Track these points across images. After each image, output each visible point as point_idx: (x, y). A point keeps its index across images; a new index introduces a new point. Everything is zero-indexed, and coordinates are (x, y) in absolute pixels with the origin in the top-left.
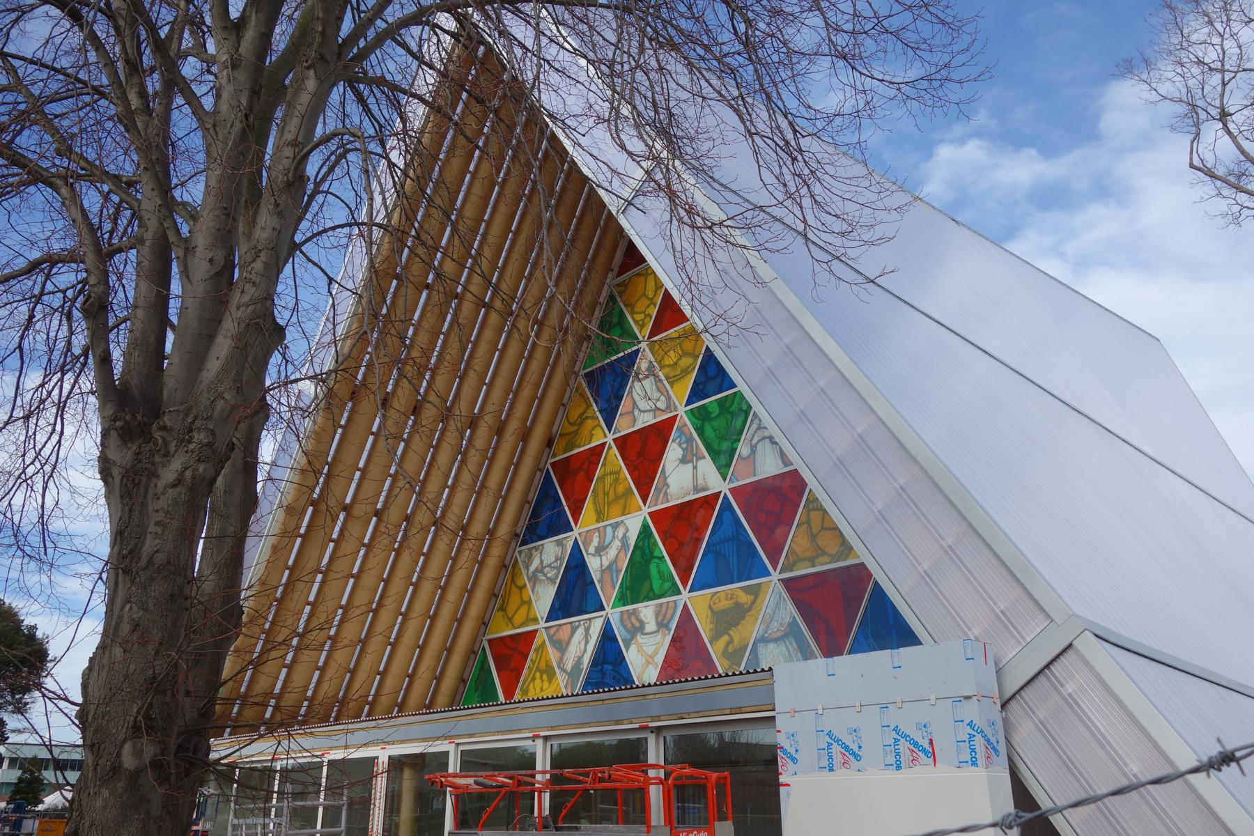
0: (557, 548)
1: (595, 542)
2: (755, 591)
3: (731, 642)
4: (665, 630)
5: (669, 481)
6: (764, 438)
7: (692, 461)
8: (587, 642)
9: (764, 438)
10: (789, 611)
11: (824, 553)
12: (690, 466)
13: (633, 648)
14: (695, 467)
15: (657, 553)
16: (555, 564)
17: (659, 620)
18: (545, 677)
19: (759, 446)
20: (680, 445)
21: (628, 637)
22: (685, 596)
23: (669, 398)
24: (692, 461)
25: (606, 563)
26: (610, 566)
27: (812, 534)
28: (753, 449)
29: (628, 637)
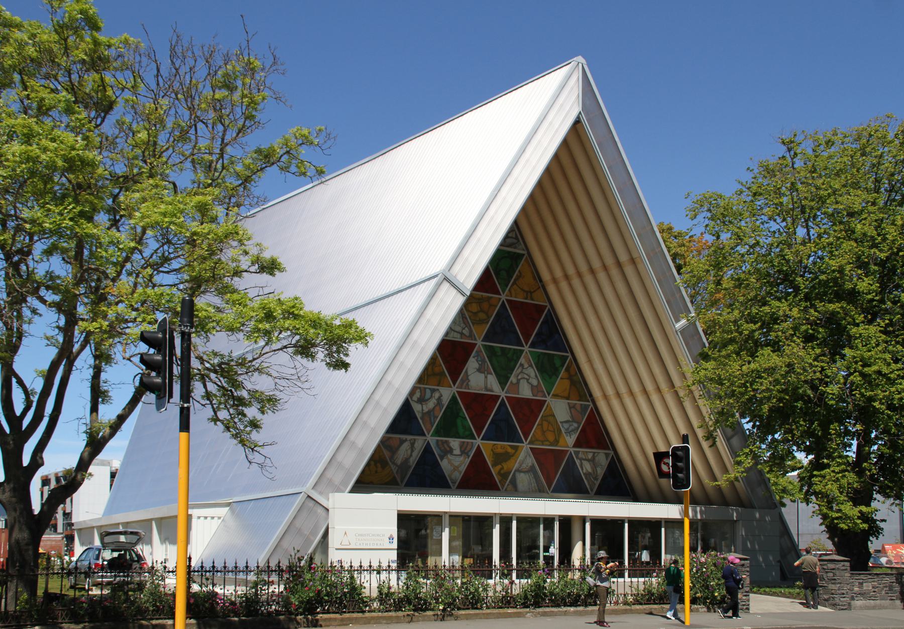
3: (502, 468)
5: (470, 378)
6: (524, 378)
7: (484, 373)
8: (412, 451)
9: (524, 378)
10: (531, 461)
11: (548, 441)
12: (483, 375)
14: (486, 377)
15: (461, 414)
18: (379, 465)
19: (521, 381)
20: (477, 361)
21: (442, 454)
22: (478, 442)
23: (471, 331)
25: (426, 409)
26: (429, 412)
28: (518, 381)
29: (442, 454)
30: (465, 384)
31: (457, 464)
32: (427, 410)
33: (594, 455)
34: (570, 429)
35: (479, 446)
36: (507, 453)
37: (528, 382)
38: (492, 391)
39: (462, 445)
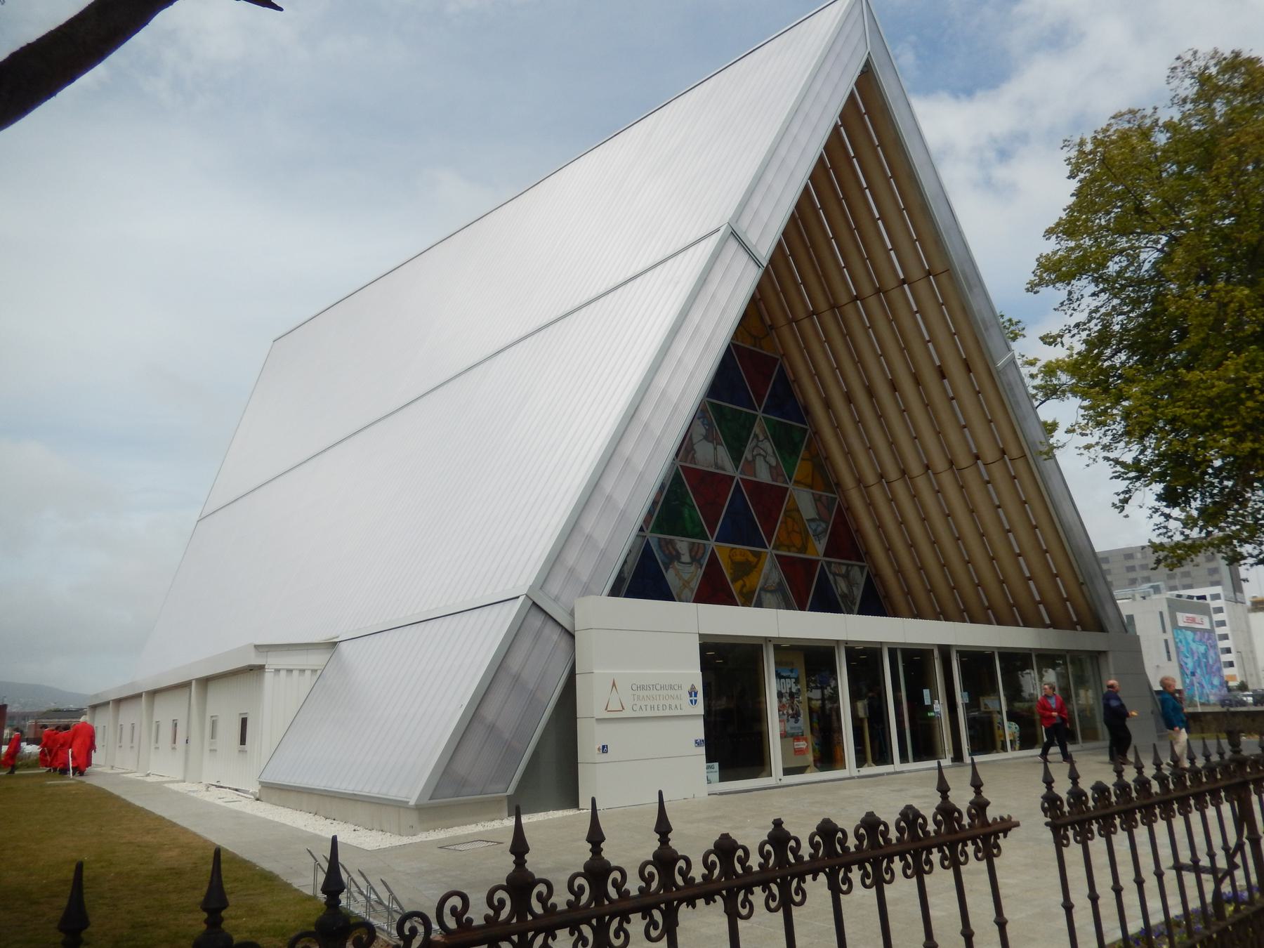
2: (758, 555)
3: (744, 585)
5: (695, 447)
6: (760, 454)
7: (712, 442)
11: (794, 546)
12: (711, 445)
13: (671, 571)
14: (715, 449)
20: (704, 425)
22: (712, 543)
28: (754, 457)
30: (690, 456)
31: (686, 577)
33: (847, 569)
34: (820, 529)
35: (713, 550)
37: (765, 461)
38: (724, 470)
39: (692, 548)
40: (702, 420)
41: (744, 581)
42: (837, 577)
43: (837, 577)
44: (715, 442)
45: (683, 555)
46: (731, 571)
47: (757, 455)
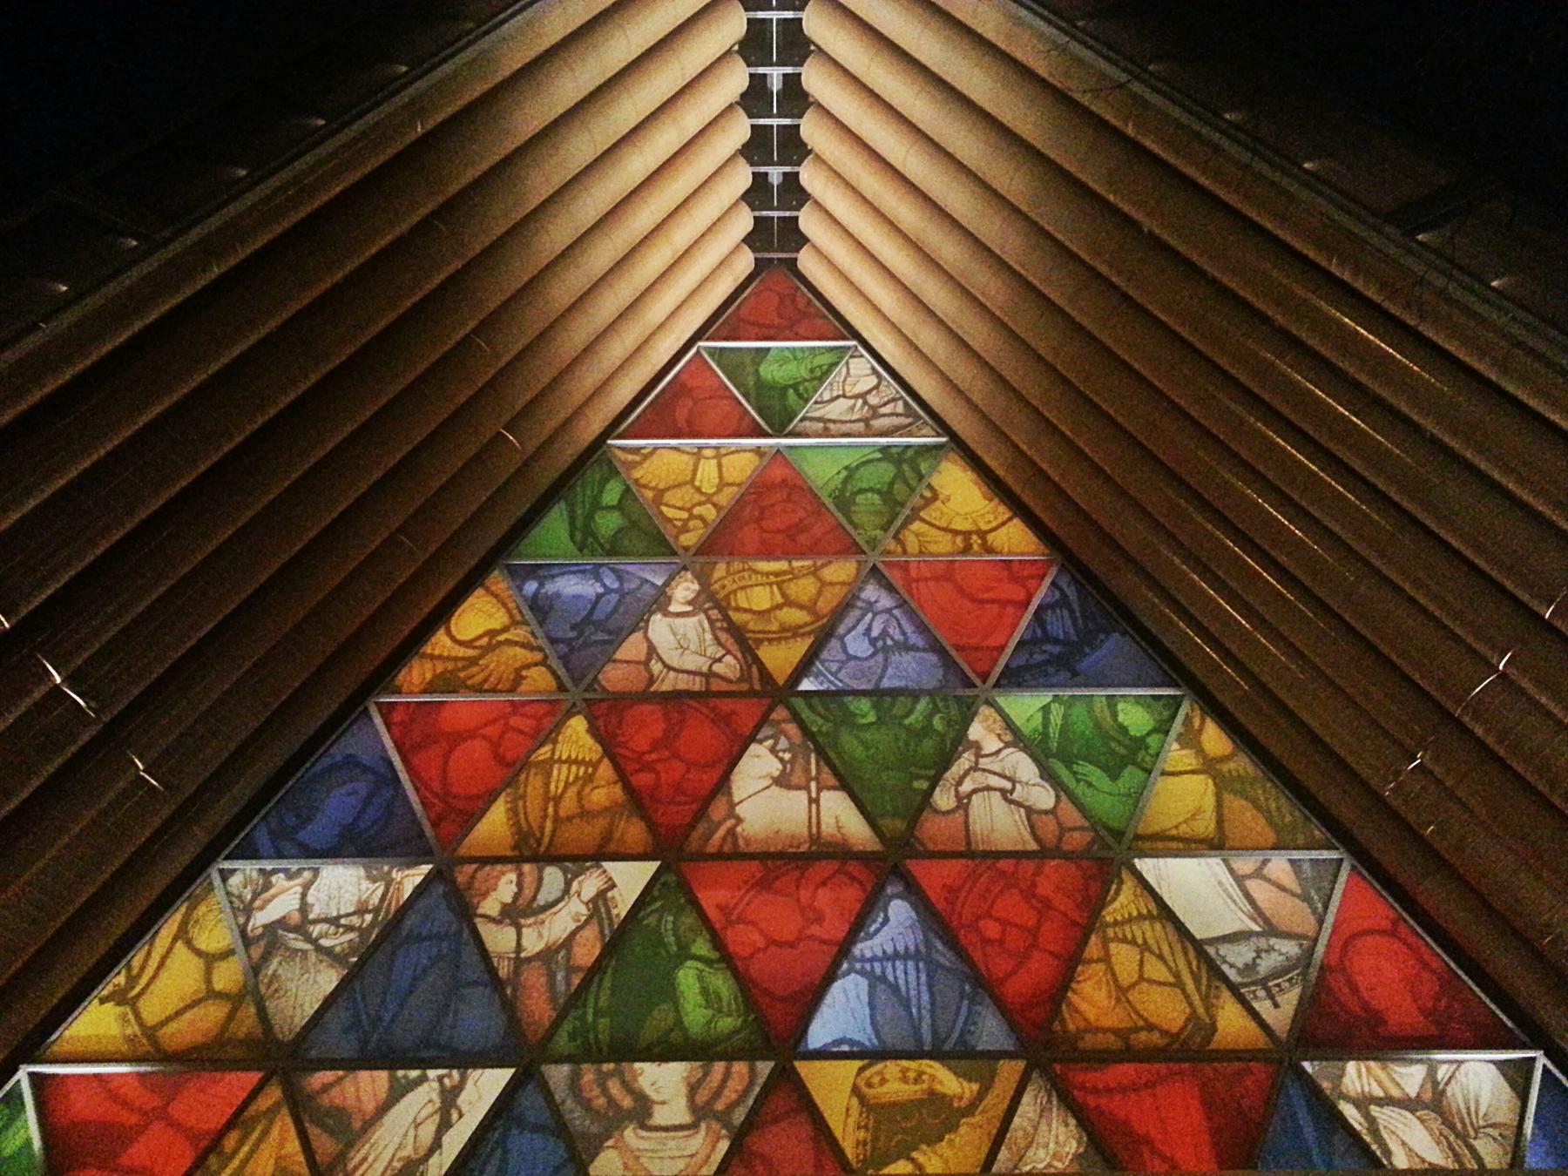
0: (365, 884)
1: (505, 888)
4: (715, 1126)
5: (739, 810)
6: (988, 788)
8: (445, 1125)
14: (814, 801)
16: (355, 920)
17: (701, 1098)
20: (773, 750)
24: (808, 789)
25: (533, 942)
26: (547, 956)
27: (1118, 987)
32: (540, 946)
36: (935, 1099)
40: (770, 742)
41: (913, 1160)
42: (1375, 1110)
43: (1375, 1110)
44: (813, 785)
45: (663, 1103)
46: (862, 1134)
47: (975, 791)
